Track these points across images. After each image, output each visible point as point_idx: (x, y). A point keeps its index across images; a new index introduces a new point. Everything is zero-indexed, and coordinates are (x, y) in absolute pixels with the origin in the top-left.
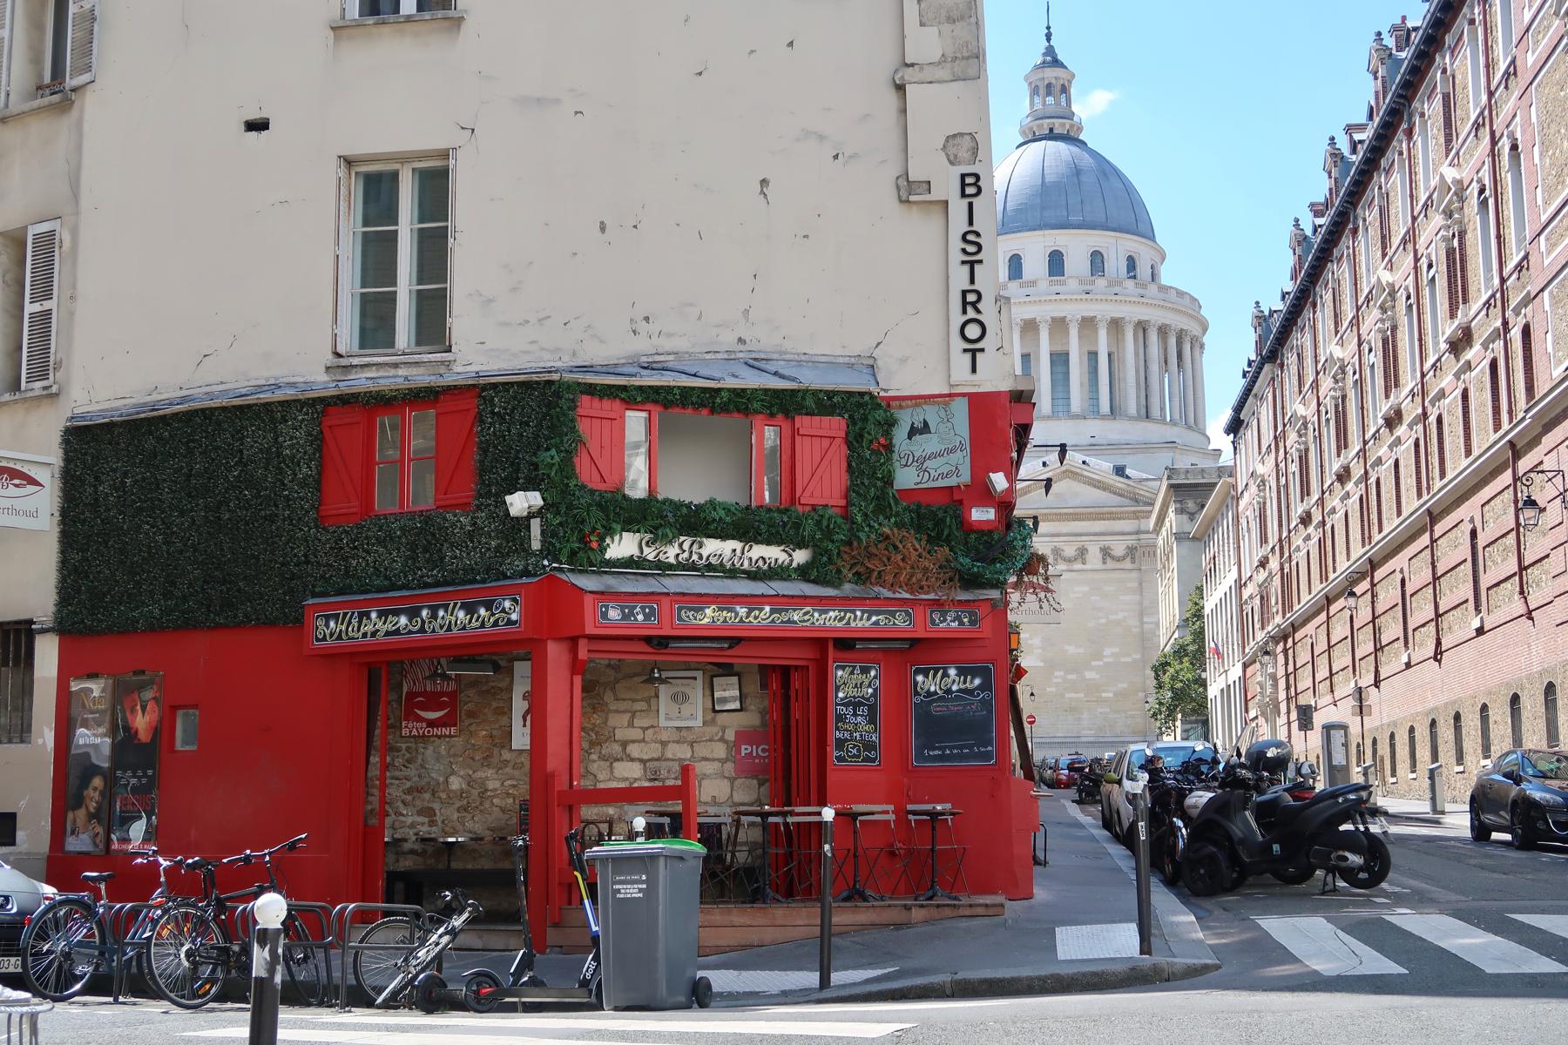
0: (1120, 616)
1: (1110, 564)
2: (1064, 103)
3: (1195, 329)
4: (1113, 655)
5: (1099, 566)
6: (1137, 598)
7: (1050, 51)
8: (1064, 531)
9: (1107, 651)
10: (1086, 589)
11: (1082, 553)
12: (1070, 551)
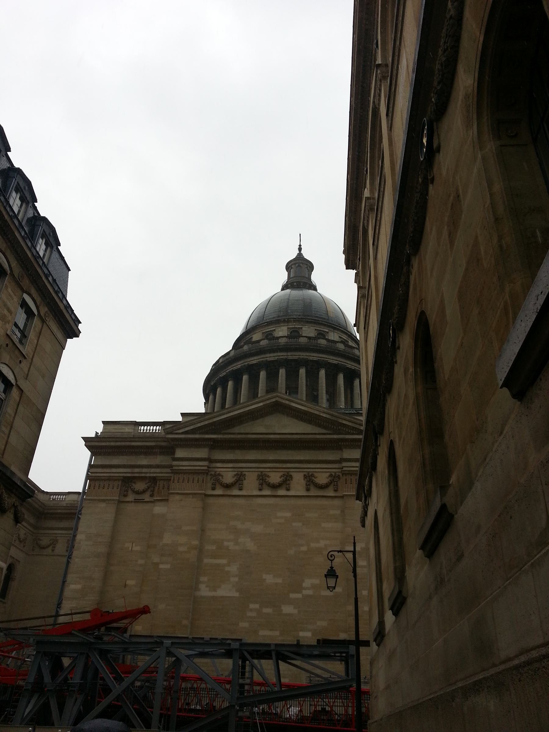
0: (322, 543)
1: (314, 492)
8: (271, 458)
9: (307, 583)
10: (288, 514)
11: (286, 482)
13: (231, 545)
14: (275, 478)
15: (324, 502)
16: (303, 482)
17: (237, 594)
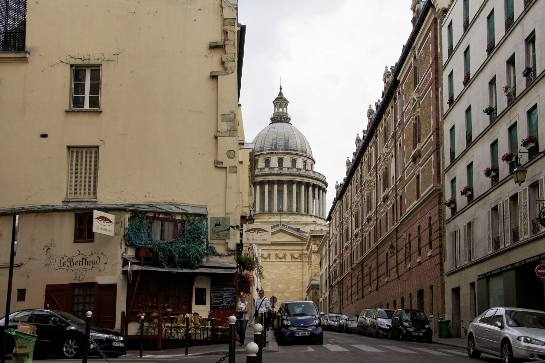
0: (296, 276)
1: (294, 260)
2: (285, 111)
3: (324, 186)
4: (293, 288)
5: (290, 260)
6: (301, 270)
7: (280, 94)
9: (292, 287)
11: (285, 256)
12: (281, 255)
13: (268, 277)
14: (281, 255)
15: (297, 263)
16: (290, 257)
17: (270, 291)
